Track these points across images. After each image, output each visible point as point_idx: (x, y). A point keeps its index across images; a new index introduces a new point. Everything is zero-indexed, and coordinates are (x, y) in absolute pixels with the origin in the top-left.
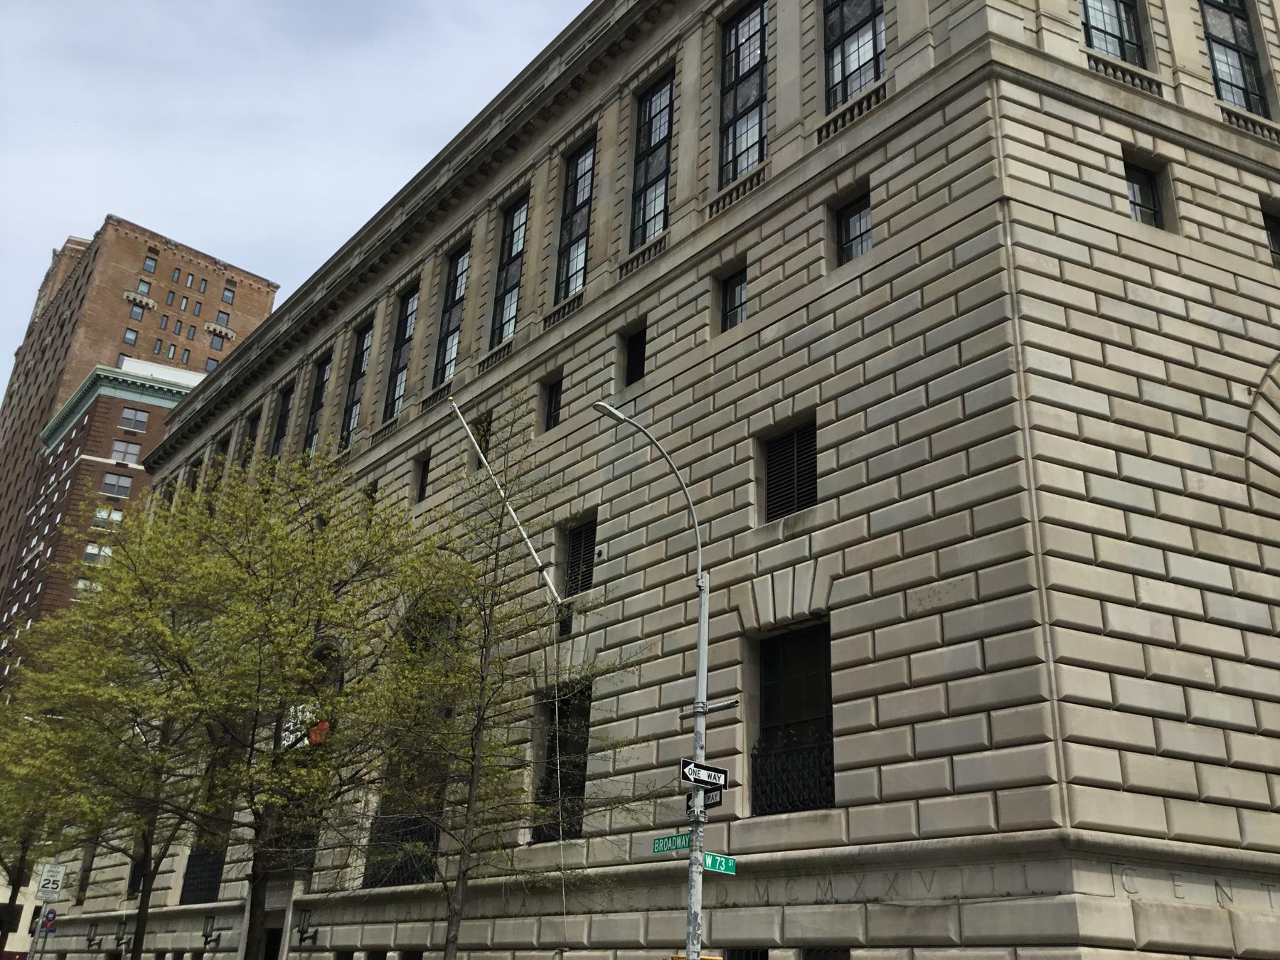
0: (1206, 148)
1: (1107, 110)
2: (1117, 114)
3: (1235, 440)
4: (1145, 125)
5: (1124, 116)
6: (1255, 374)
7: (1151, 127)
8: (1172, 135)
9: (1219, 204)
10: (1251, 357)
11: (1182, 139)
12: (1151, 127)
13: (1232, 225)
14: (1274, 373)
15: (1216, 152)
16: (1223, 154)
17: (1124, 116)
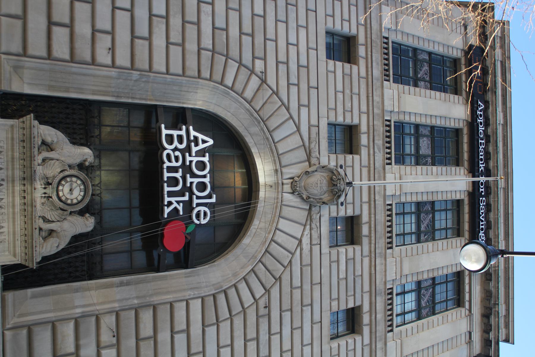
0: (370, 92)
1: (369, 30)
2: (369, 36)
3: (234, 52)
4: (369, 53)
5: (369, 40)
6: (271, 80)
7: (369, 56)
8: (370, 69)
9: (348, 91)
10: (280, 82)
11: (370, 77)
12: (369, 56)
13: (340, 96)
14: (275, 96)
15: (371, 98)
16: (371, 103)
17: (369, 40)
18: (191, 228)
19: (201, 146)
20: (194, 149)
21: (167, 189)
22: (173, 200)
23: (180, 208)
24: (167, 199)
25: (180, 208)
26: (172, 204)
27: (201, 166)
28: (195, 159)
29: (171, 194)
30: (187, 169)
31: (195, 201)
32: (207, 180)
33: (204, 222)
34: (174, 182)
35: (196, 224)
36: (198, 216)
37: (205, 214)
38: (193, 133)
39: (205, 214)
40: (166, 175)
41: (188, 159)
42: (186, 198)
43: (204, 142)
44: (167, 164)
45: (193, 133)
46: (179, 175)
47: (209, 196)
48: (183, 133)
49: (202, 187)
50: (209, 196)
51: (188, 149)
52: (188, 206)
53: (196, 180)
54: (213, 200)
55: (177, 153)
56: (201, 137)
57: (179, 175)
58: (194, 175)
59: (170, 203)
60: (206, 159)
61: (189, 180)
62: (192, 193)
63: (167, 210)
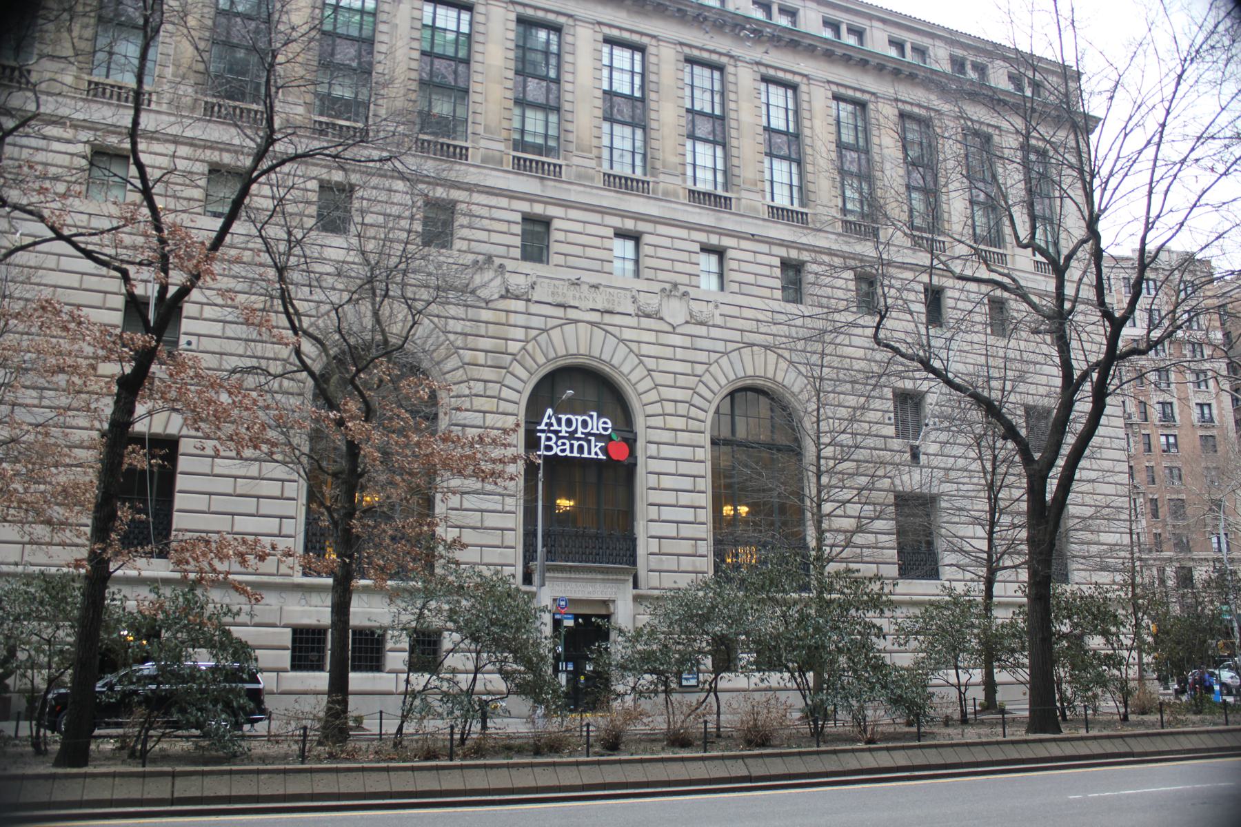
18: (614, 436)
19: (553, 421)
20: (556, 427)
21: (585, 455)
22: (593, 450)
23: (600, 445)
24: (593, 456)
25: (600, 445)
26: (595, 451)
27: (569, 423)
28: (564, 428)
29: (589, 453)
30: (572, 436)
31: (595, 431)
32: (580, 418)
33: (610, 425)
34: (581, 448)
35: (613, 430)
36: (605, 429)
37: (605, 423)
38: (543, 427)
39: (605, 423)
40: (576, 454)
41: (563, 434)
42: (593, 439)
43: (550, 417)
44: (567, 453)
45: (543, 427)
46: (576, 444)
47: (591, 417)
48: (543, 436)
49: (585, 424)
50: (591, 417)
51: (556, 432)
52: (599, 437)
53: (580, 429)
54: (595, 414)
55: (559, 443)
56: (546, 420)
57: (576, 444)
58: (576, 431)
59: (596, 454)
60: (564, 417)
61: (579, 435)
62: (590, 434)
63: (601, 456)
